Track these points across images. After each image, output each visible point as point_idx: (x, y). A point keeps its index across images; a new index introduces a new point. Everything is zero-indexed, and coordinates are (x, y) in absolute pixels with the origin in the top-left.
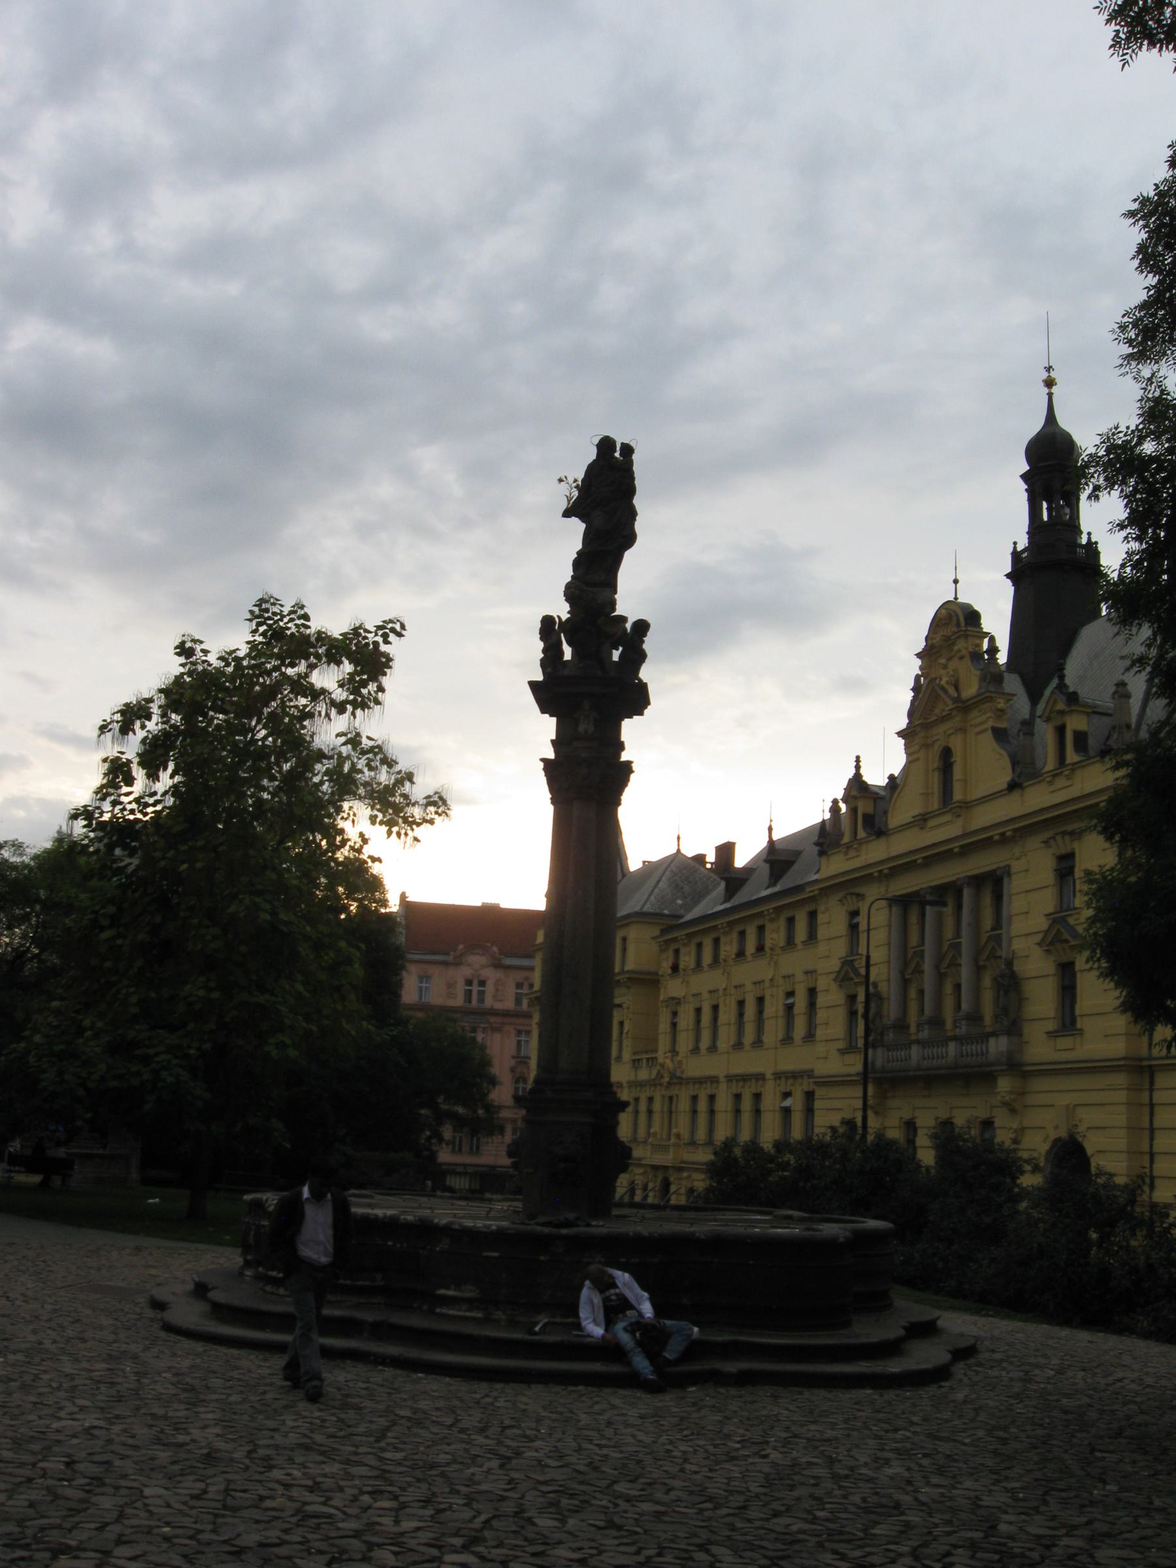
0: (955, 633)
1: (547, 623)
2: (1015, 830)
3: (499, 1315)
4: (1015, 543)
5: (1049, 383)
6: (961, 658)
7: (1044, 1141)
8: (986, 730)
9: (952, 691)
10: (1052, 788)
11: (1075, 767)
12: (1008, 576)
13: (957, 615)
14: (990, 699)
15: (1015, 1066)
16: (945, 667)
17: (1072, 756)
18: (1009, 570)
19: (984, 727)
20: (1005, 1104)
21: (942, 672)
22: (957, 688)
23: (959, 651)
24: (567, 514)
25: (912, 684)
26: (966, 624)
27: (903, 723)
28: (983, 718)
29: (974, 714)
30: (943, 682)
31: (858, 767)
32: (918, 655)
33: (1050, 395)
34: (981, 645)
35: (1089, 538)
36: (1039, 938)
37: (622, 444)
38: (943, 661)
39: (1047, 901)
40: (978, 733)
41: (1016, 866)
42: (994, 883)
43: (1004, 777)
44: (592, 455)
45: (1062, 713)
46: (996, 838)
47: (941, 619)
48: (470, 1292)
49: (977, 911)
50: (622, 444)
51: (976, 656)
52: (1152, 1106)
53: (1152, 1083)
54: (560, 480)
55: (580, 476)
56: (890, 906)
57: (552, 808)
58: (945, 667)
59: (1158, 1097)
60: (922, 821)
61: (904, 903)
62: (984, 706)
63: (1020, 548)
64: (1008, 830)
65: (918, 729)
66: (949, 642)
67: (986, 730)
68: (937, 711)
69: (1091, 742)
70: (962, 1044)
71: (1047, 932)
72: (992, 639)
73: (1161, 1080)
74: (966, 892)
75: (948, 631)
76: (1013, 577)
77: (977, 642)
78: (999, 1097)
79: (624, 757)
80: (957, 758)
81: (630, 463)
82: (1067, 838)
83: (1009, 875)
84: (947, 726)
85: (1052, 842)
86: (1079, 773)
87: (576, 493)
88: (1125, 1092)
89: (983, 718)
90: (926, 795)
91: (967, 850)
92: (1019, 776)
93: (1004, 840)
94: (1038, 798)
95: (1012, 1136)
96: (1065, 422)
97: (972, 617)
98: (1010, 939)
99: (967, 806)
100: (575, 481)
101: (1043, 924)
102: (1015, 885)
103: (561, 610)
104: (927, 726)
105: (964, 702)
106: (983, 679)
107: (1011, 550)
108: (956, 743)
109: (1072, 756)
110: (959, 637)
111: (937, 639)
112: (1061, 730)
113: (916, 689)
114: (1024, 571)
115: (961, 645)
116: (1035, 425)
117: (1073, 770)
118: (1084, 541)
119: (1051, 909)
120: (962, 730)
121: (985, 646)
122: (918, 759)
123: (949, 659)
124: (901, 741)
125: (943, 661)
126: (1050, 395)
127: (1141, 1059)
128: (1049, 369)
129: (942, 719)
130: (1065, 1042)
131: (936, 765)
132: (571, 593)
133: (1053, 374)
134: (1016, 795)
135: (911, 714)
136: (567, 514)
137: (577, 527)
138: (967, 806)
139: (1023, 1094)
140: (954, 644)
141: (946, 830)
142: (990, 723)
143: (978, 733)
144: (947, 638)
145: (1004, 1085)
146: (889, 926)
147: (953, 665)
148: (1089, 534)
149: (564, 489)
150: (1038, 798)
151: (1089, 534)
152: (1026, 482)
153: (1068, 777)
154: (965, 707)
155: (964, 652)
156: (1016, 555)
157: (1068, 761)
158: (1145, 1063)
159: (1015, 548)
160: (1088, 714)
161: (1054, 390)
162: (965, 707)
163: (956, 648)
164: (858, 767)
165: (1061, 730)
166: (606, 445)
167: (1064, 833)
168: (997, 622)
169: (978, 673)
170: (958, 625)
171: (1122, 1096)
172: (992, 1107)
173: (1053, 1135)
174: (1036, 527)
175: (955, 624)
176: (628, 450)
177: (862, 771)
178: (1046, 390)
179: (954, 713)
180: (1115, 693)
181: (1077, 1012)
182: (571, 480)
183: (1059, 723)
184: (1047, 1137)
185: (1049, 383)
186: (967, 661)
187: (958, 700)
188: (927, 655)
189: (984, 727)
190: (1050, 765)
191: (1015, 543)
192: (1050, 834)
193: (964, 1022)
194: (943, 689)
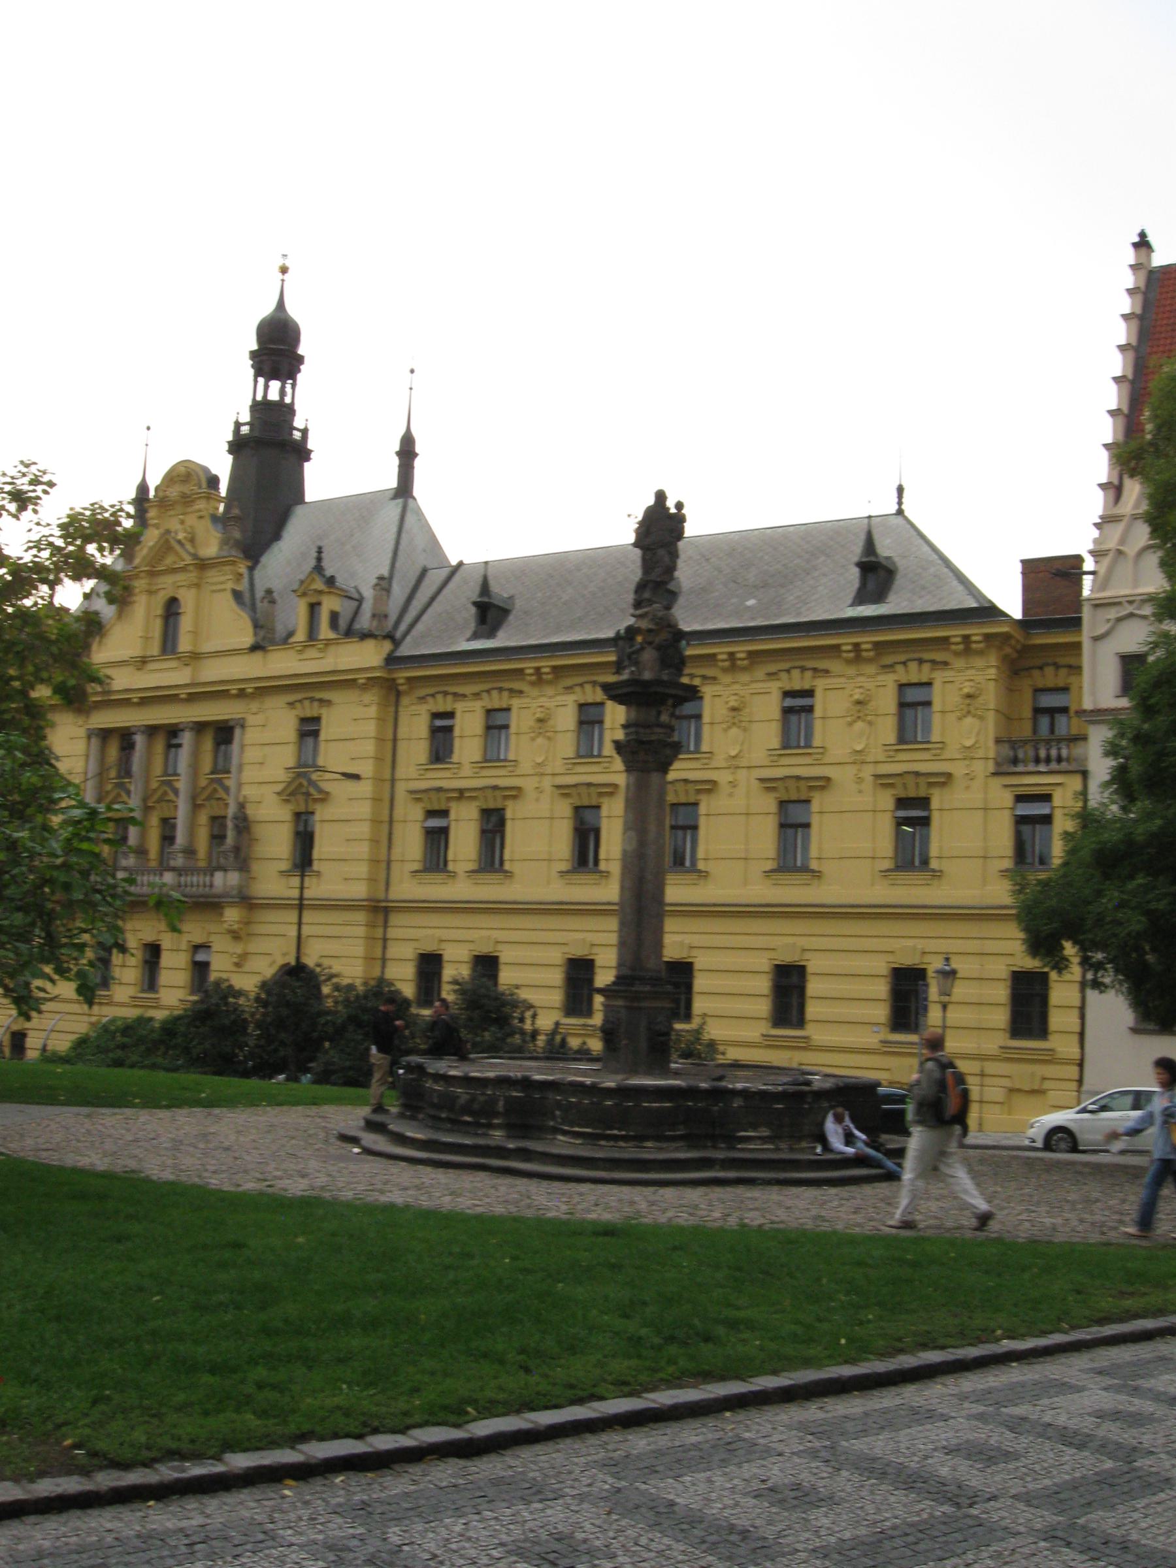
2: (256, 688)
3: (783, 1146)
5: (284, 270)
7: (271, 965)
11: (328, 643)
14: (234, 563)
15: (247, 902)
17: (325, 632)
19: (223, 587)
20: (230, 932)
23: (200, 511)
28: (222, 579)
33: (283, 280)
36: (279, 787)
39: (287, 756)
41: (251, 720)
42: (224, 733)
43: (248, 640)
44: (651, 501)
45: (320, 592)
46: (234, 692)
48: (765, 1132)
49: (196, 754)
52: (385, 940)
53: (386, 922)
56: (89, 737)
59: (392, 933)
60: (142, 662)
61: (105, 735)
64: (249, 688)
70: (180, 875)
71: (290, 783)
73: (395, 919)
74: (186, 738)
75: (186, 489)
76: (238, 446)
78: (225, 926)
82: (316, 704)
83: (243, 727)
84: (180, 577)
85: (298, 705)
86: (332, 649)
88: (363, 928)
89: (222, 579)
90: (146, 639)
91: (193, 698)
93: (242, 694)
94: (282, 663)
95: (236, 960)
96: (294, 311)
98: (240, 785)
99: (195, 657)
102: (251, 735)
106: (224, 542)
108: (188, 599)
109: (325, 632)
112: (314, 607)
115: (201, 505)
116: (267, 308)
119: (291, 765)
120: (197, 586)
127: (379, 901)
129: (174, 571)
134: (258, 656)
138: (195, 657)
139: (248, 923)
141: (172, 676)
142: (230, 585)
144: (184, 496)
145: (232, 915)
146: (87, 756)
147: (191, 520)
150: (282, 663)
156: (238, 425)
157: (322, 637)
158: (384, 904)
161: (286, 277)
162: (203, 565)
165: (314, 607)
167: (312, 699)
171: (361, 931)
172: (160, 932)
173: (281, 961)
179: (191, 568)
180: (376, 585)
181: (316, 854)
183: (313, 600)
184: (274, 962)
185: (284, 270)
187: (195, 556)
189: (223, 587)
190: (300, 636)
192: (299, 696)
193: (180, 855)
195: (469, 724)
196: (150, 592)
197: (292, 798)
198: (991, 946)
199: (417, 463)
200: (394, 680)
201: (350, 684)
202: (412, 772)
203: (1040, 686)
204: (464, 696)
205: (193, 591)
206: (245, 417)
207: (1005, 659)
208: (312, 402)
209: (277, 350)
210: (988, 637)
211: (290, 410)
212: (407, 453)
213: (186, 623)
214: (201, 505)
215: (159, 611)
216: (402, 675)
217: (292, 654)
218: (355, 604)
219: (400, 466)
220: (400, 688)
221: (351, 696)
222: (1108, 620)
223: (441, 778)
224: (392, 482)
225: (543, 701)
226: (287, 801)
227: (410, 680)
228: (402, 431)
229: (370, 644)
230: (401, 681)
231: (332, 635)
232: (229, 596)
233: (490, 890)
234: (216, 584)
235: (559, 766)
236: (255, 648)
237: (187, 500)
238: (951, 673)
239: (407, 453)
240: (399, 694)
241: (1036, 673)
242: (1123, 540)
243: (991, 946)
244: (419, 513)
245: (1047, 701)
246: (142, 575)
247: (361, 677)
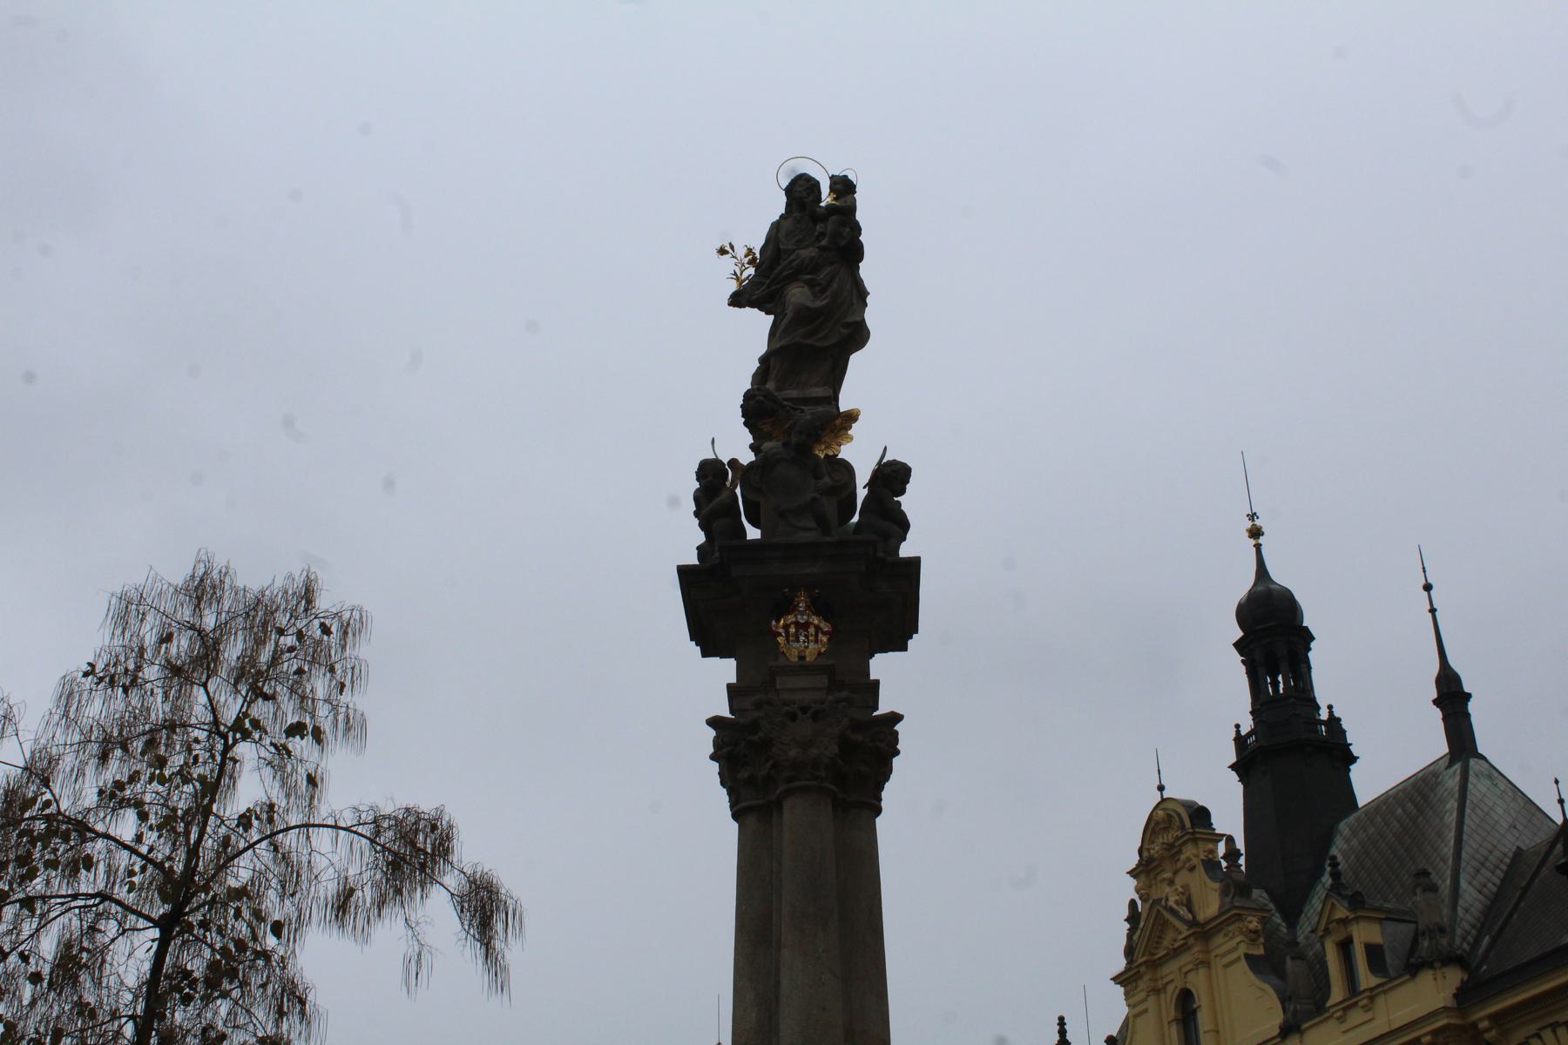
0: (1178, 838)
1: (711, 474)
4: (1237, 726)
5: (1255, 533)
6: (1192, 869)
8: (1238, 959)
9: (1183, 911)
10: (1344, 1027)
11: (1373, 994)
12: (1233, 767)
13: (1179, 815)
14: (1239, 917)
16: (1171, 882)
17: (1366, 979)
18: (1233, 759)
19: (1233, 956)
21: (1168, 889)
22: (1189, 906)
23: (1189, 860)
24: (737, 300)
25: (1126, 913)
26: (1193, 825)
27: (1120, 964)
28: (1233, 943)
29: (1219, 939)
30: (1171, 903)
31: (1062, 1032)
32: (1132, 873)
33: (1258, 547)
34: (1213, 851)
35: (1331, 713)
37: (832, 178)
38: (1167, 875)
40: (1226, 966)
44: (777, 206)
45: (1345, 922)
47: (1157, 823)
50: (832, 178)
51: (1211, 865)
54: (722, 251)
55: (757, 243)
57: (734, 827)
58: (1171, 882)
62: (1231, 928)
63: (1244, 731)
65: (1143, 969)
66: (1173, 851)
67: (1238, 959)
68: (1165, 943)
72: (1230, 840)
75: (1168, 838)
76: (1241, 768)
77: (1211, 846)
79: (884, 708)
80: (1202, 1000)
81: (852, 209)
84: (1185, 959)
86: (1380, 1001)
87: (751, 271)
89: (1233, 943)
96: (1280, 575)
97: (1201, 815)
100: (750, 250)
103: (738, 446)
104: (1154, 965)
105: (1203, 925)
106: (1224, 892)
107: (1233, 735)
108: (1198, 983)
109: (1366, 979)
110: (1185, 843)
111: (1156, 849)
112: (1345, 946)
113: (1133, 917)
114: (1250, 760)
115: (1189, 851)
116: (1244, 583)
117: (1372, 999)
118: (1324, 715)
120: (1206, 964)
121: (1221, 848)
122: (1146, 1011)
123: (1175, 873)
124: (1120, 990)
125: (1167, 875)
126: (1258, 547)
128: (1252, 516)
129: (1175, 953)
131: (1173, 1014)
132: (756, 410)
133: (1257, 522)
135: (1129, 951)
136: (737, 300)
137: (756, 326)
140: (1180, 852)
142: (1243, 949)
143: (1226, 966)
144: (1171, 846)
148: (1330, 707)
149: (728, 264)
151: (1330, 707)
153: (1366, 1008)
154: (1204, 932)
155: (1195, 861)
156: (1240, 740)
157: (1363, 987)
159: (1238, 732)
160: (1380, 920)
161: (1261, 540)
162: (1204, 932)
163: (1183, 857)
164: (1062, 1032)
165: (1345, 946)
166: (801, 190)
168: (1229, 817)
169: (1217, 886)
170: (1183, 827)
174: (1262, 704)
175: (1175, 829)
176: (844, 187)
177: (1068, 1037)
178: (1253, 542)
179: (1191, 941)
182: (741, 252)
183: (1340, 936)
185: (1255, 533)
186: (1200, 872)
187: (1193, 923)
188: (1145, 870)
189: (1233, 956)
191: (1237, 726)
194: (1172, 911)
196: (1157, 991)
200: (1474, 1025)
205: (1202, 971)
206: (1247, 725)
208: (1333, 681)
212: (1452, 696)
213: (1204, 1020)
214: (1189, 851)
215: (1172, 1012)
216: (1481, 1015)
217: (1332, 1023)
219: (1444, 719)
220: (1487, 1036)
224: (1440, 747)
227: (1494, 1018)
228: (1434, 668)
229: (1426, 979)
230: (1484, 1024)
231: (1374, 981)
232: (1243, 965)
234: (1224, 955)
237: (1173, 851)
239: (1452, 696)
244: (1494, 774)
246: (1143, 969)
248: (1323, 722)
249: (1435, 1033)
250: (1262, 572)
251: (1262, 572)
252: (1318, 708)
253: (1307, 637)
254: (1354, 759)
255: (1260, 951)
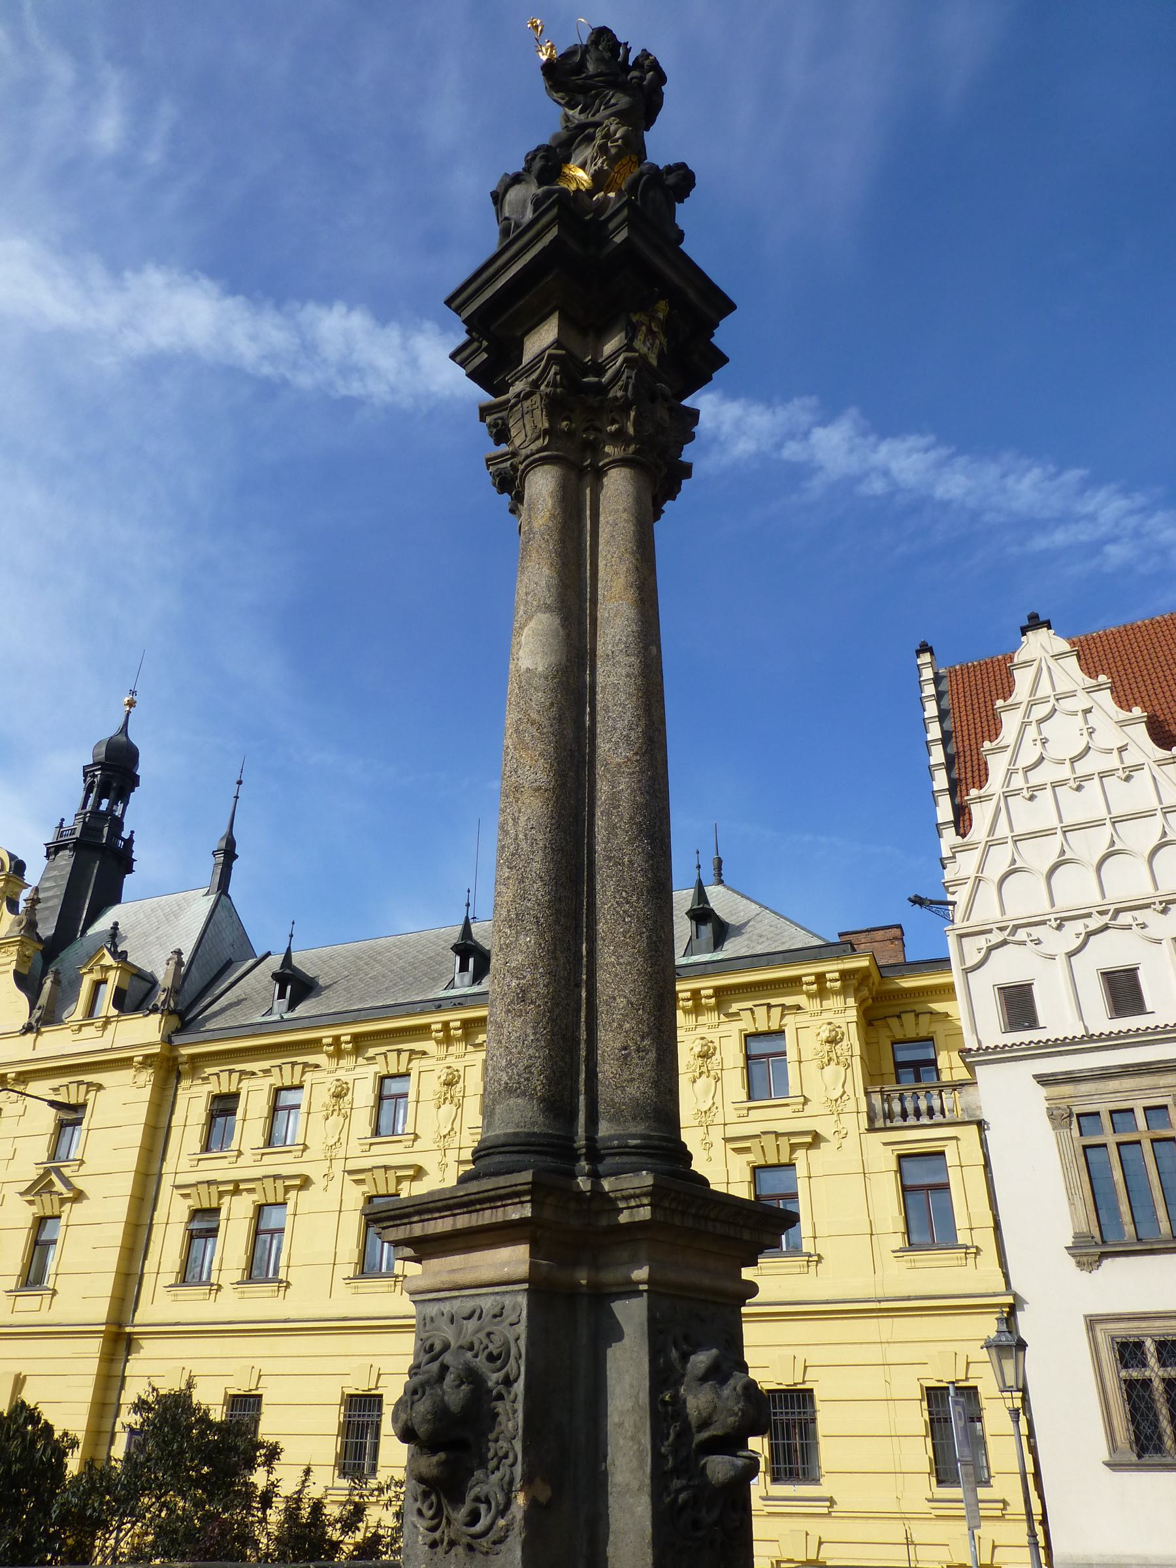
4: (63, 820)
11: (107, 1021)
34: (18, 894)
43: (23, 1019)
69: (127, 1001)
92: (37, 1021)
94: (57, 1043)
96: (135, 737)
101: (34, 1174)
116: (109, 730)
130: (29, 1302)
134: (30, 1037)
148: (132, 832)
151: (132, 832)
152: (85, 775)
191: (63, 820)
192: (65, 1080)
195: (254, 1103)
197: (37, 1198)
198: (895, 1354)
199: (235, 864)
201: (124, 1063)
202: (185, 1164)
203: (899, 1036)
204: (254, 1074)
207: (861, 1003)
209: (115, 771)
210: (845, 975)
211: (118, 824)
218: (150, 985)
221: (126, 1075)
222: (979, 950)
223: (219, 1168)
225: (341, 1074)
226: (31, 1203)
227: (193, 1058)
228: (224, 831)
233: (261, 1304)
235: (355, 1148)
236: (28, 1029)
238: (806, 1017)
240: (179, 1076)
241: (894, 1022)
242: (981, 867)
243: (895, 1354)
245: (904, 1055)
247: (138, 1055)
248: (123, 839)
249: (146, 1057)
250: (124, 729)
251: (124, 729)
252: (122, 829)
253: (135, 781)
254: (131, 871)
255: (25, 971)
